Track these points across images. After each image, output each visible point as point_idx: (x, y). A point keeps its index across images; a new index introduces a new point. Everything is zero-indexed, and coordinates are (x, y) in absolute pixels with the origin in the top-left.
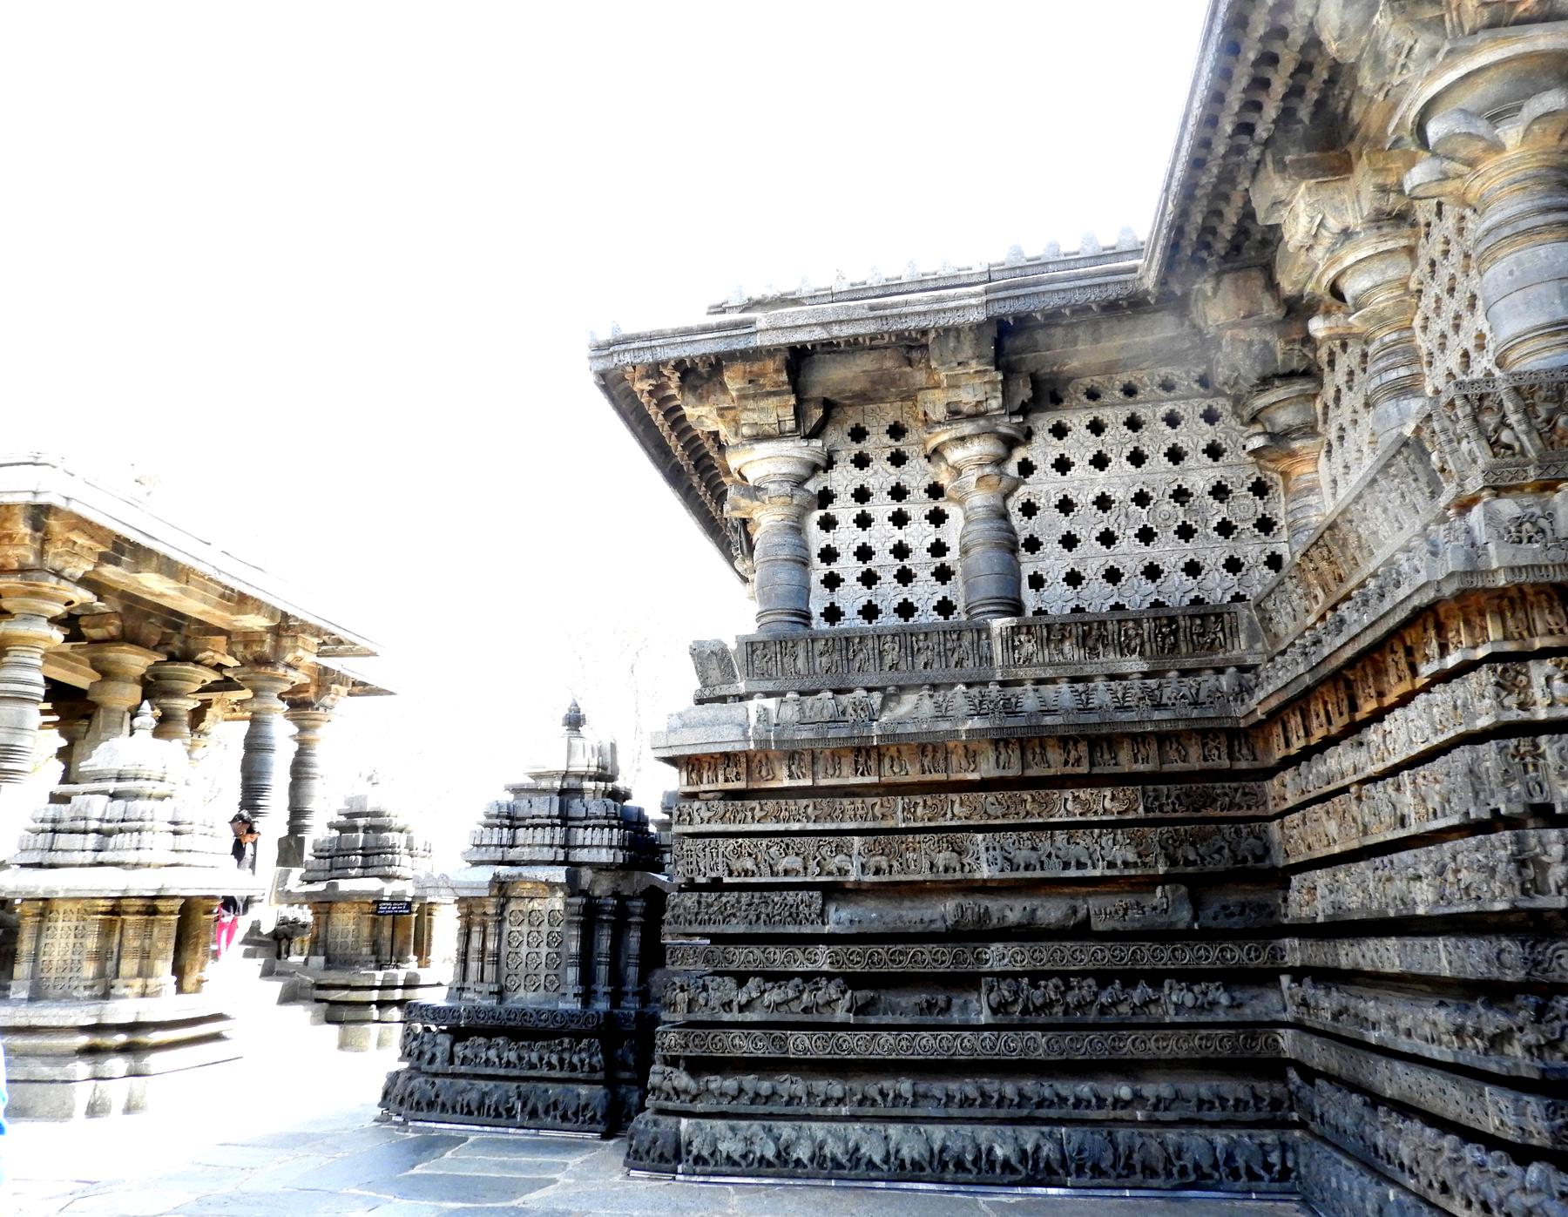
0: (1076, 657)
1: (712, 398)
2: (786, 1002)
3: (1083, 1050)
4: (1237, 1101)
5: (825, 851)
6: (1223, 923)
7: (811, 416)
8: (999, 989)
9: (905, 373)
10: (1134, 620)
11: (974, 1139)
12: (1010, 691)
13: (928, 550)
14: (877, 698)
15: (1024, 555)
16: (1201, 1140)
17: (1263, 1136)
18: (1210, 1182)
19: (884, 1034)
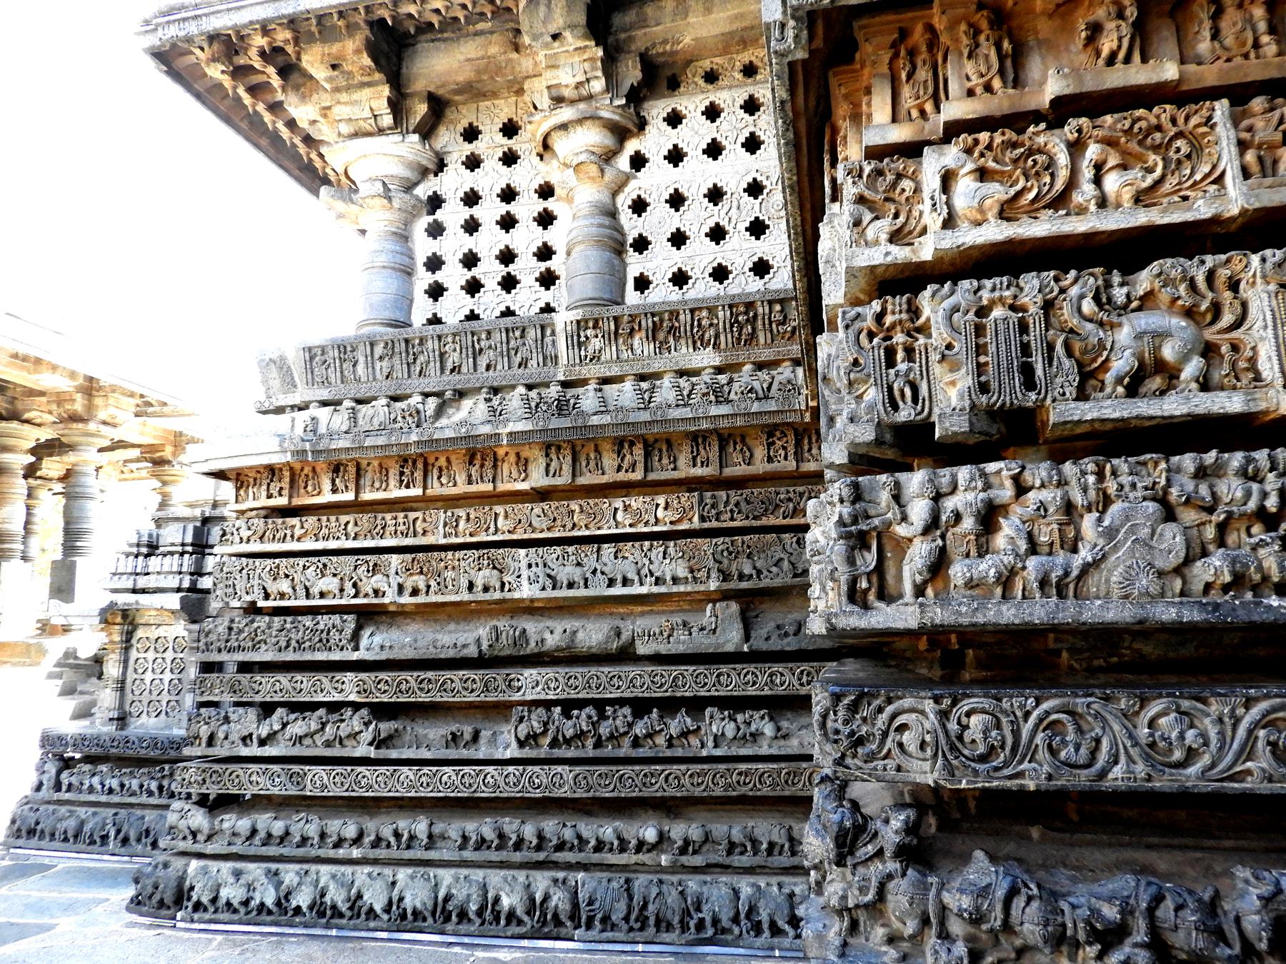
0: (646, 353)
1: (315, 96)
2: (312, 735)
3: (612, 786)
4: (771, 845)
5: (310, 572)
6: (776, 644)
7: (415, 112)
8: (530, 719)
9: (511, 60)
10: (708, 308)
11: (484, 888)
12: (571, 392)
13: (535, 254)
14: (432, 403)
15: (632, 256)
16: (725, 890)
17: (795, 884)
18: (730, 937)
19: (405, 769)
